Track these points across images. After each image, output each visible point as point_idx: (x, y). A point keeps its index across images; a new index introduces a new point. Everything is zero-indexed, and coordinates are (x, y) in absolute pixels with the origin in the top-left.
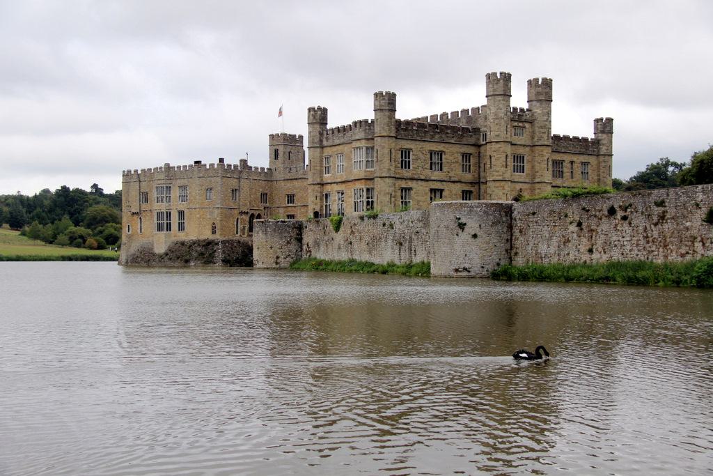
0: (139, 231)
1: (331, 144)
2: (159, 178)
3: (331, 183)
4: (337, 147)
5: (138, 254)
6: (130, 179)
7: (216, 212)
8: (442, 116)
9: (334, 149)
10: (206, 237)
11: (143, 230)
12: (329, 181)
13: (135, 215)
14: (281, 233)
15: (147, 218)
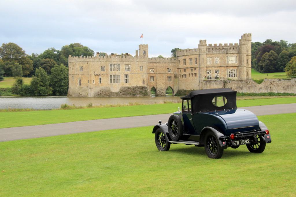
0: (99, 83)
1: (211, 53)
2: (114, 60)
3: (211, 67)
4: (215, 55)
5: (101, 92)
6: (94, 60)
7: (145, 75)
8: (220, 45)
9: (213, 55)
10: (140, 86)
11: (101, 82)
12: (210, 66)
13: (97, 77)
14: (221, 84)
15: (105, 77)
